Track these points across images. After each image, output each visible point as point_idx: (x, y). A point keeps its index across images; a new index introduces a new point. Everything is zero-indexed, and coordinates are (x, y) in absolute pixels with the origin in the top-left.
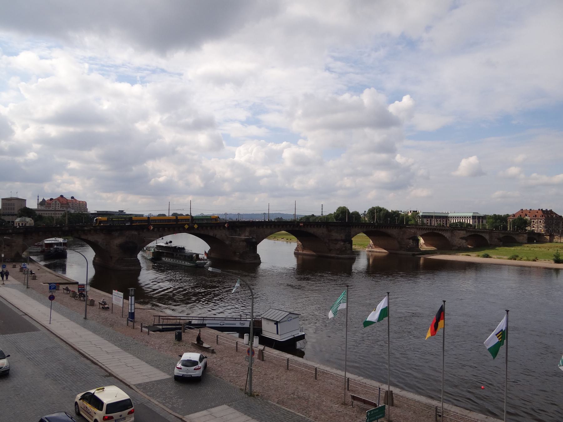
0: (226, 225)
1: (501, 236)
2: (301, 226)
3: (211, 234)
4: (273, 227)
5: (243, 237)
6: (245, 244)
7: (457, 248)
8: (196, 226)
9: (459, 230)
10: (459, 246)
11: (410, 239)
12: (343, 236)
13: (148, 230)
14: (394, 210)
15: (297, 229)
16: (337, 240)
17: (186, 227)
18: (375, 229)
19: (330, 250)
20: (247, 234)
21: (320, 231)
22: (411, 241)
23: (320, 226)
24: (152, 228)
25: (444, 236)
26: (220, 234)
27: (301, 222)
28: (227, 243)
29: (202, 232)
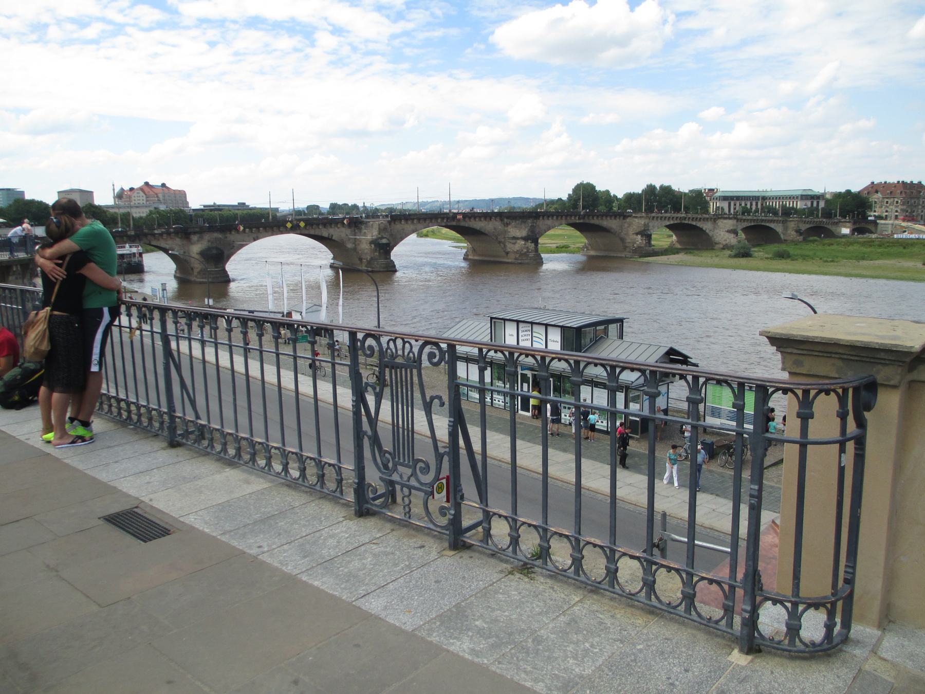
0: (345, 222)
2: (459, 220)
4: (415, 221)
7: (721, 246)
8: (302, 224)
10: (724, 243)
11: (637, 234)
12: (524, 233)
13: (238, 231)
17: (289, 225)
18: (581, 221)
19: (507, 253)
22: (639, 236)
24: (242, 228)
25: (701, 229)
26: (337, 233)
29: (312, 232)
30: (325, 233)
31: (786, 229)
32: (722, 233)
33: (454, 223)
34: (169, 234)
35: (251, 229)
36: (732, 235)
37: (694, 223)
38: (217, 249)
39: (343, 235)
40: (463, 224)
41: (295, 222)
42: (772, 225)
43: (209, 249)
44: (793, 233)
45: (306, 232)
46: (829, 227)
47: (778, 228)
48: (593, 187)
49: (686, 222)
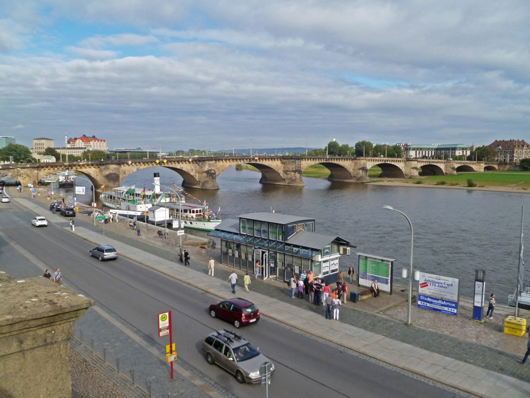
0: (190, 160)
1: (456, 166)
2: (256, 160)
6: (205, 174)
8: (165, 161)
10: (410, 175)
11: (360, 169)
13: (128, 164)
17: (157, 161)
18: (328, 162)
22: (361, 171)
23: (275, 159)
24: (130, 163)
25: (397, 167)
29: (170, 166)
30: (178, 166)
31: (446, 167)
33: (253, 162)
34: (88, 165)
35: (135, 163)
36: (415, 170)
37: (393, 163)
38: (115, 174)
39: (189, 168)
40: (258, 162)
42: (438, 165)
43: (110, 174)
44: (450, 169)
45: (168, 166)
46: (471, 166)
47: (442, 166)
49: (388, 162)
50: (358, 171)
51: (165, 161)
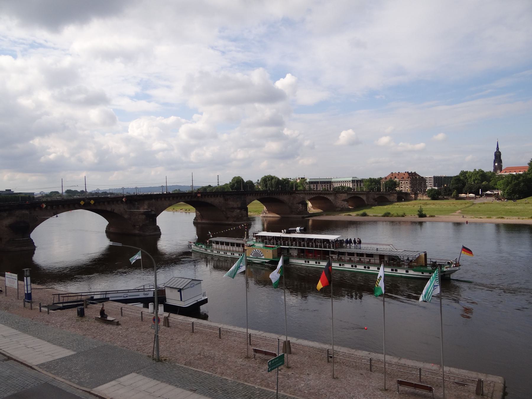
0: (124, 200)
1: (376, 196)
2: (199, 197)
3: (109, 209)
4: (171, 199)
5: (142, 210)
7: (340, 209)
8: (92, 202)
9: (341, 193)
11: (299, 203)
12: (238, 204)
13: (41, 208)
14: (285, 178)
15: (195, 199)
16: (233, 208)
17: (82, 203)
19: (228, 218)
20: (146, 207)
21: (217, 201)
22: (300, 205)
23: (217, 196)
24: (44, 206)
25: (328, 200)
26: (118, 208)
27: (199, 193)
28: (126, 216)
29: (99, 208)
31: (368, 198)
32: (340, 202)
41: (87, 201)
46: (386, 196)
48: (482, 171)
50: (298, 205)
51: (92, 202)
